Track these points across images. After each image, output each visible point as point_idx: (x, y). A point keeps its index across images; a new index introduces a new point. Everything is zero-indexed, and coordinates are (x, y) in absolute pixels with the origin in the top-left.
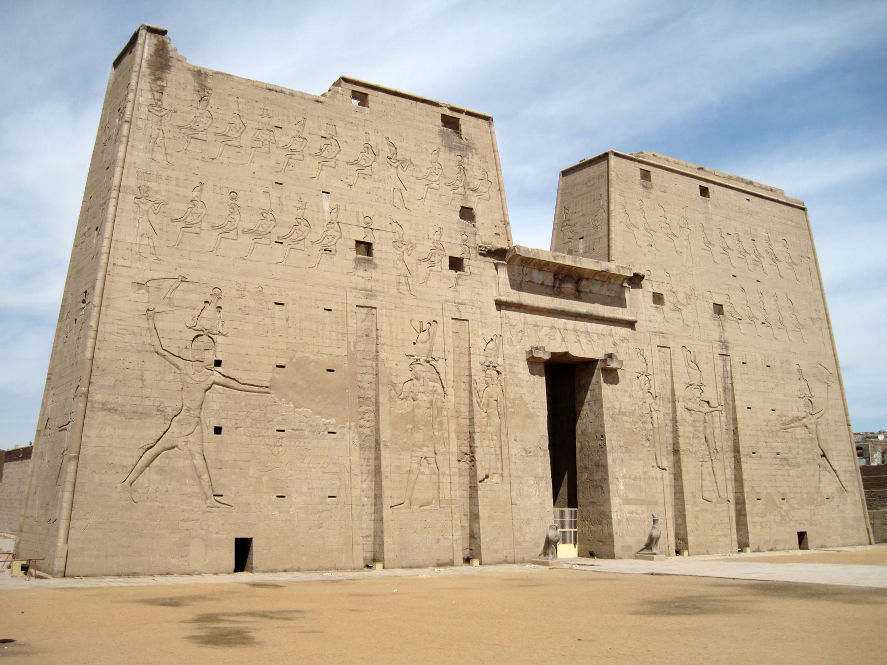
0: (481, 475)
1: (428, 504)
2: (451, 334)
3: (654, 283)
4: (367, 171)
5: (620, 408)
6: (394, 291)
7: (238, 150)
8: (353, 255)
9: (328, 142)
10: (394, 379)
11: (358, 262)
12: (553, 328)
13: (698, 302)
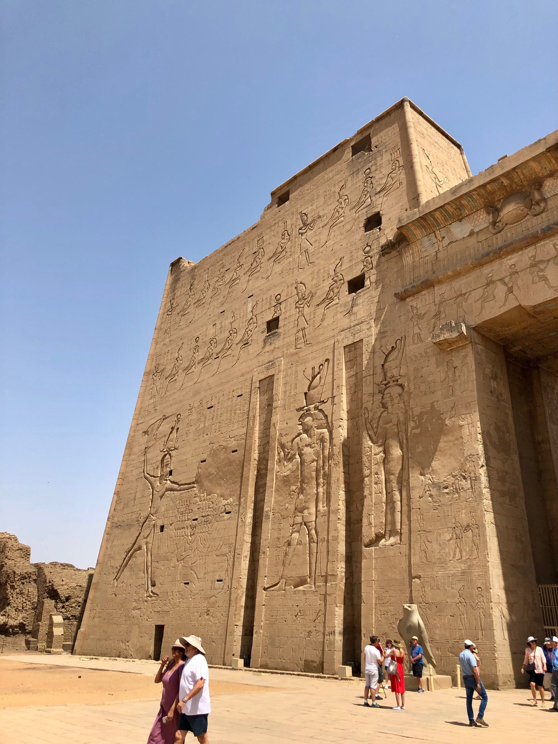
0: (368, 532)
1: (303, 582)
4: (284, 253)
6: (292, 350)
9: (257, 254)
10: (284, 440)
11: (265, 341)
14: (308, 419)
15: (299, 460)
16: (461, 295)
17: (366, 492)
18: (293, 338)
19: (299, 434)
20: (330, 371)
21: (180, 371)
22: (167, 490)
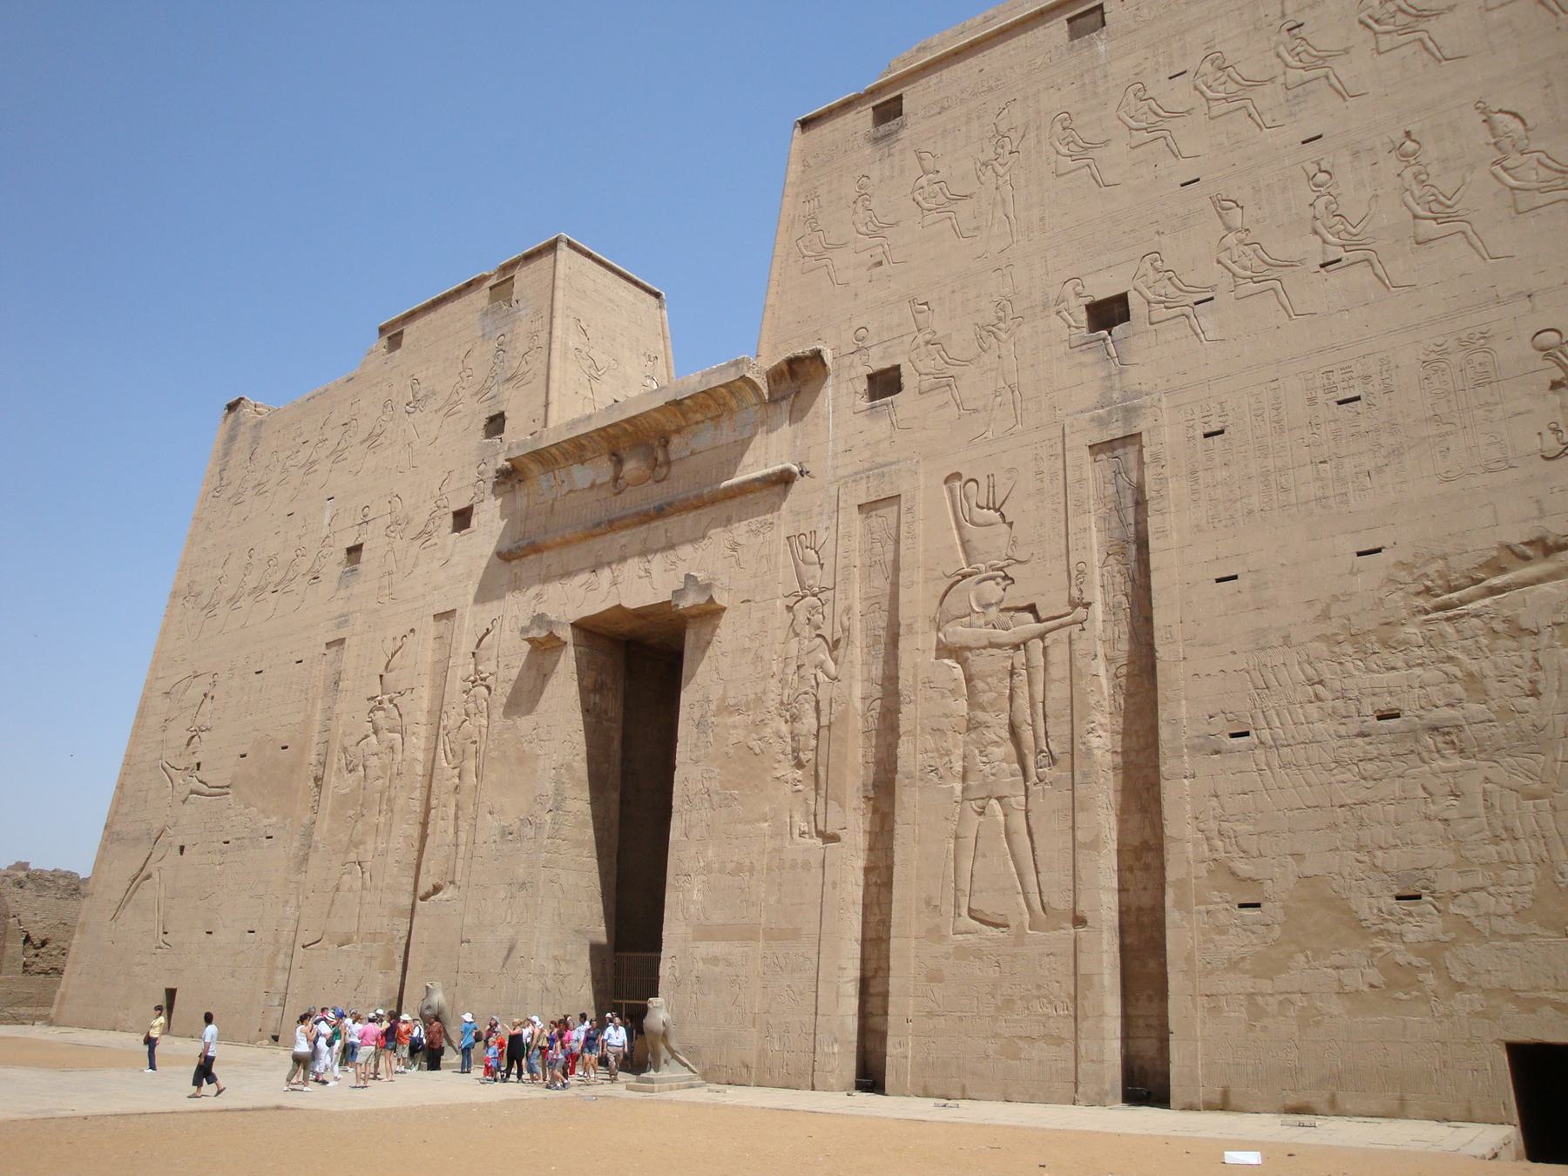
1: (348, 941)
3: (872, 351)
5: (724, 698)
10: (350, 742)
13: (1026, 330)
15: (362, 773)
19: (367, 736)
21: (223, 602)
22: (192, 792)
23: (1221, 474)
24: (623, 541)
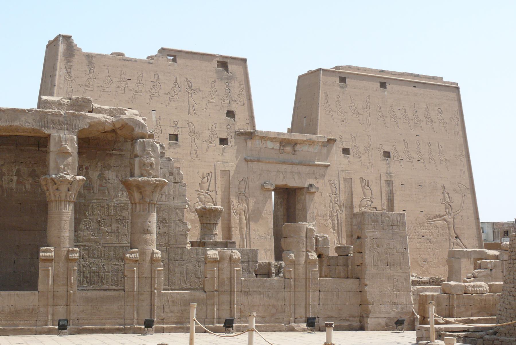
2: (219, 178)
4: (176, 97)
5: (318, 213)
7: (109, 93)
8: (168, 141)
9: (155, 84)
12: (278, 171)
14: (202, 196)
16: (269, 171)
17: (233, 233)
18: (189, 152)
20: (213, 178)
23: (404, 192)
24: (285, 167)
